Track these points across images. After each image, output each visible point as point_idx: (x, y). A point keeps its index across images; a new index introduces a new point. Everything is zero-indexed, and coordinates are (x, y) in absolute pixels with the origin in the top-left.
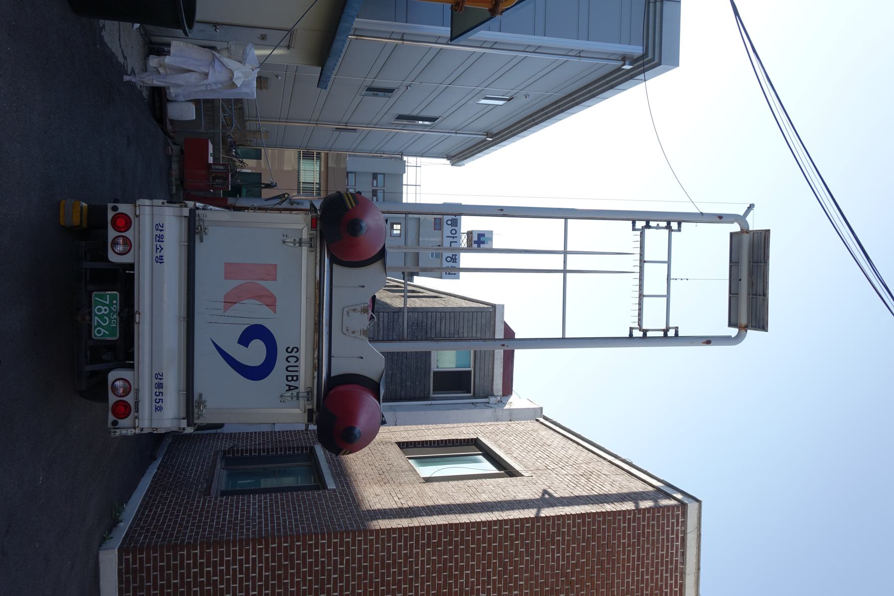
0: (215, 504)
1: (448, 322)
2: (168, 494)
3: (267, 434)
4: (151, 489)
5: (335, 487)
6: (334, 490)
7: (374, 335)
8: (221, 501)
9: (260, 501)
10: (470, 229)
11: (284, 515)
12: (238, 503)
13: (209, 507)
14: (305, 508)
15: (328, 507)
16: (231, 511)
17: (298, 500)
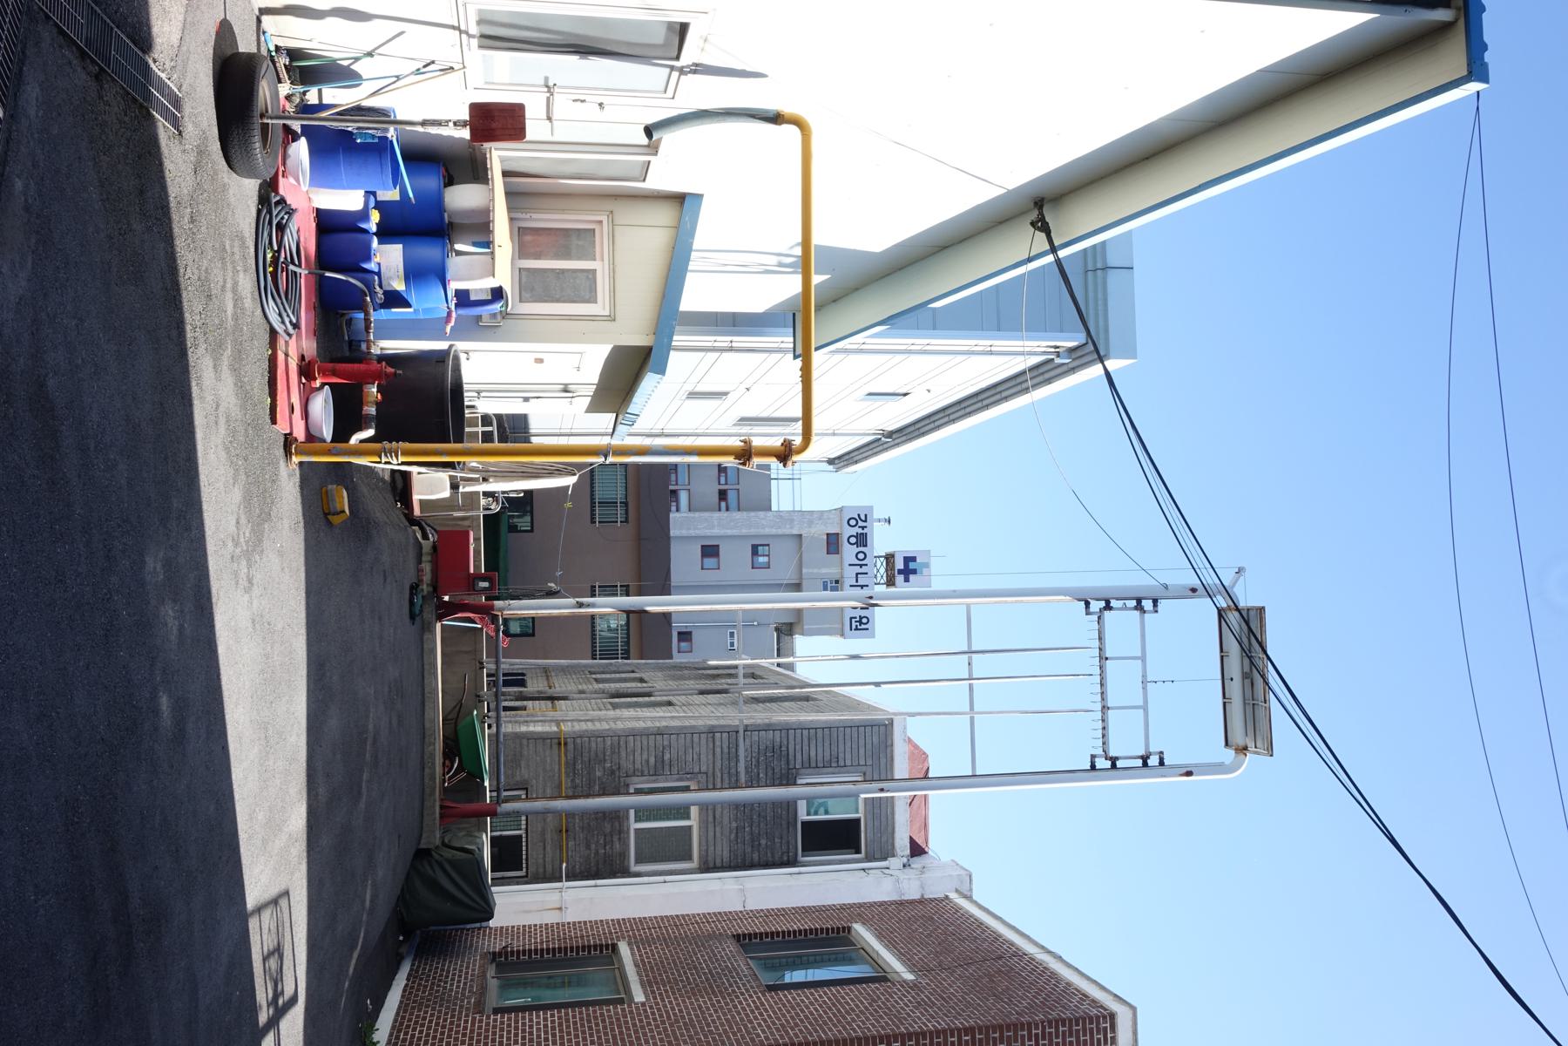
0: (488, 1024)
1: (819, 744)
2: (426, 1012)
3: (552, 927)
4: (403, 1007)
5: (644, 1000)
6: (643, 1004)
7: (708, 768)
8: (495, 1021)
9: (545, 1019)
10: (889, 550)
11: (577, 1036)
12: (516, 1022)
13: (480, 1028)
14: (605, 1027)
15: (634, 1025)
16: (509, 1032)
17: (595, 1018)
